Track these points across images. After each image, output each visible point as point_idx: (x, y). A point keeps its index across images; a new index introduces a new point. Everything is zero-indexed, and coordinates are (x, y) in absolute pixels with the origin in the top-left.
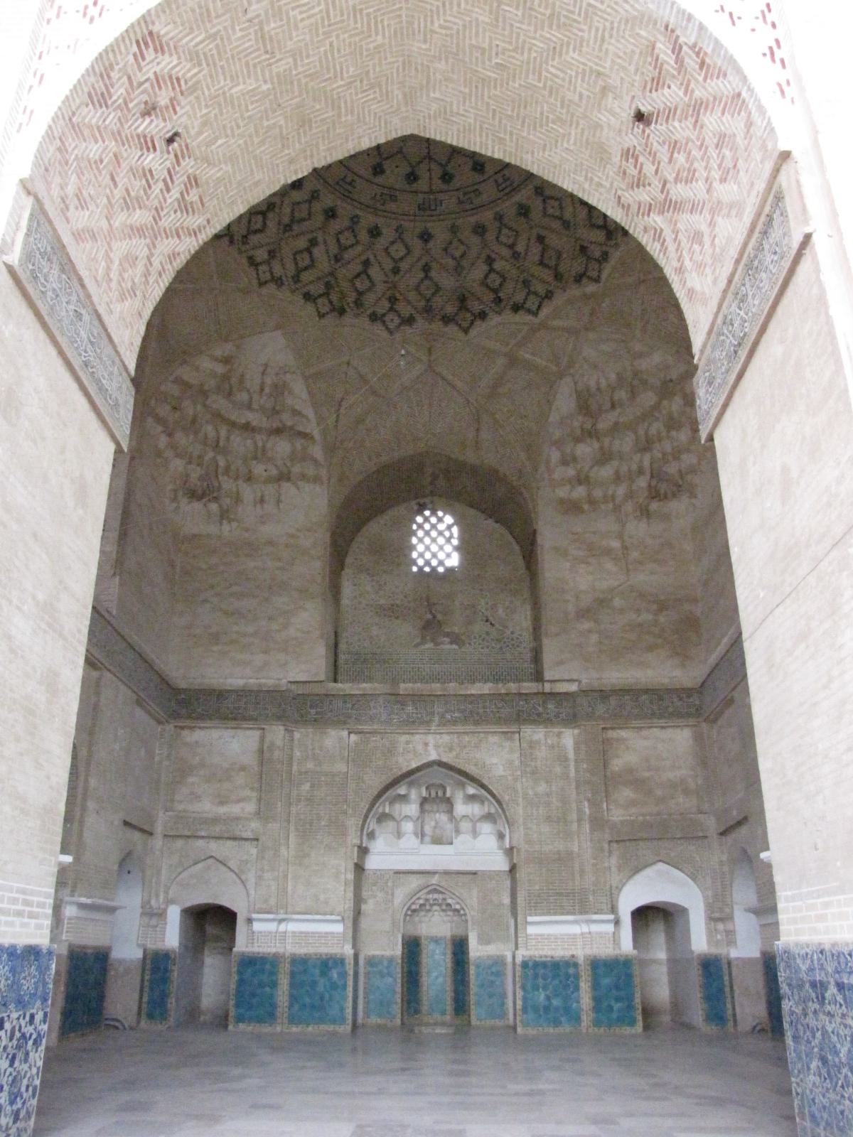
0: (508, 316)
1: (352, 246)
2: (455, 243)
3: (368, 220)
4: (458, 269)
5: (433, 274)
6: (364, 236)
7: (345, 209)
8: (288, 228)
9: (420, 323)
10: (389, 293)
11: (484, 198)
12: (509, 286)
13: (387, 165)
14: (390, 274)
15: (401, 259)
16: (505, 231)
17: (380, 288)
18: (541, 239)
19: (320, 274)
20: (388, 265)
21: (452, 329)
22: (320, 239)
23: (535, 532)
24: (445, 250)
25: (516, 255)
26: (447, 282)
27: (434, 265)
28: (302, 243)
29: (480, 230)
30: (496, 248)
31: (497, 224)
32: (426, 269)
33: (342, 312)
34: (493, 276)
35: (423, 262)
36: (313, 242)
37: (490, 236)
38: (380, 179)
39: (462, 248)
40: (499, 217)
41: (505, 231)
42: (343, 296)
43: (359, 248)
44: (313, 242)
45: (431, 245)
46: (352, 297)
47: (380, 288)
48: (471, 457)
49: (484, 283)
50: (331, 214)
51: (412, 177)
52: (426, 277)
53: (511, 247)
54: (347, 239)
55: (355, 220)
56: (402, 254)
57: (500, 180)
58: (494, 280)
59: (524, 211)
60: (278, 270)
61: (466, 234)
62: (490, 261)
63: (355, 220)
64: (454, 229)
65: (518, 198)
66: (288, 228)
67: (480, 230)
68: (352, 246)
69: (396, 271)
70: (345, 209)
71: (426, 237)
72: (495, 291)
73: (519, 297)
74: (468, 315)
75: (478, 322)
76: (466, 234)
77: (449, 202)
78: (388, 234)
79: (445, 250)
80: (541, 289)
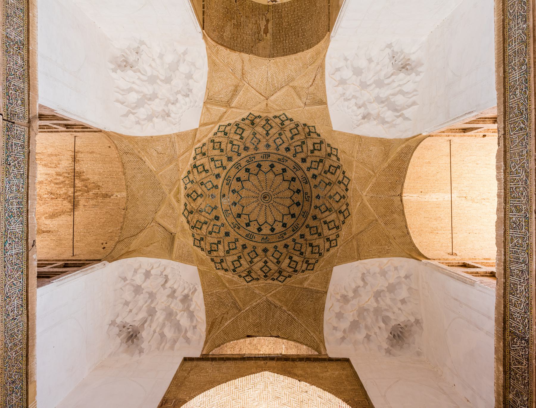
0: (232, 122)
1: (297, 146)
2: (256, 144)
3: (289, 155)
4: (254, 134)
5: (265, 132)
6: (292, 148)
7: (298, 160)
8: (321, 161)
9: (271, 116)
10: (283, 126)
11: (245, 160)
12: (233, 130)
13: (281, 172)
14: (283, 133)
15: (278, 138)
16: (236, 150)
17: (287, 129)
18: (222, 151)
19: (312, 140)
20: (283, 137)
21: (257, 114)
22: (309, 152)
23: (203, 28)
24: (260, 141)
25: (231, 142)
26: (259, 129)
27: (265, 136)
28: (316, 153)
29: (246, 149)
30: (239, 143)
31: (239, 152)
32: (267, 134)
33: (305, 125)
34: (240, 133)
35: (269, 136)
36: (312, 152)
37: (242, 147)
38: (284, 167)
39: (253, 141)
40: (239, 155)
41: (236, 150)
42: (304, 129)
43: (294, 144)
44: (312, 152)
45: (265, 143)
46: (300, 128)
47: (287, 129)
48: (246, 56)
49: (243, 130)
50: (304, 160)
51: (272, 166)
52: (267, 131)
53: (233, 145)
54: (299, 149)
55: (295, 156)
56: (277, 140)
57: (240, 168)
58: (239, 131)
59: (230, 159)
60: (329, 149)
61: (252, 147)
62: (242, 138)
63: (295, 156)
64: (256, 149)
65: (233, 163)
66: (321, 161)
67: (246, 149)
68: (297, 146)
69: (280, 134)
70: (298, 160)
71: (268, 146)
72: (238, 127)
73: (228, 128)
74: (250, 119)
75: (245, 117)
76: (252, 147)
77: (258, 158)
78: (282, 148)
79: (260, 141)
80: (219, 134)
